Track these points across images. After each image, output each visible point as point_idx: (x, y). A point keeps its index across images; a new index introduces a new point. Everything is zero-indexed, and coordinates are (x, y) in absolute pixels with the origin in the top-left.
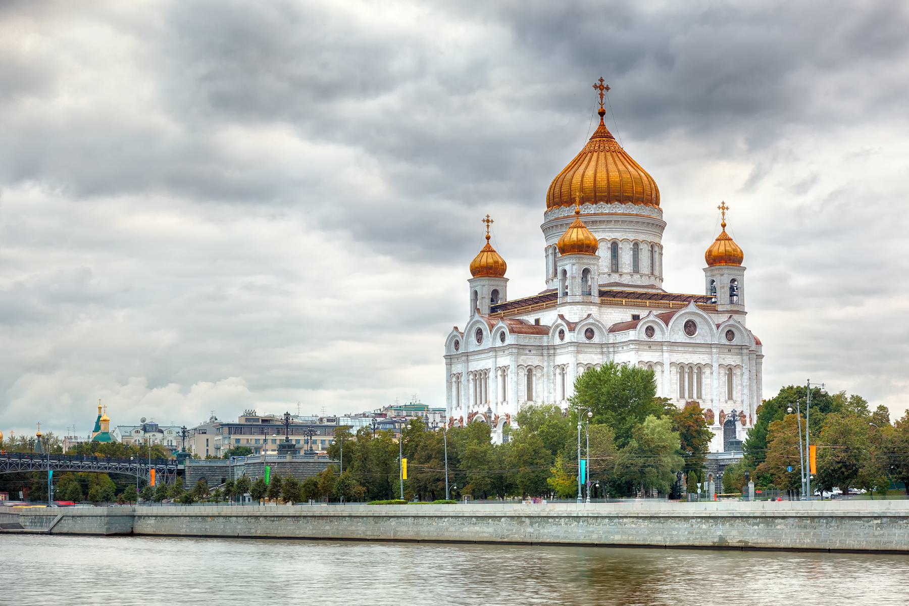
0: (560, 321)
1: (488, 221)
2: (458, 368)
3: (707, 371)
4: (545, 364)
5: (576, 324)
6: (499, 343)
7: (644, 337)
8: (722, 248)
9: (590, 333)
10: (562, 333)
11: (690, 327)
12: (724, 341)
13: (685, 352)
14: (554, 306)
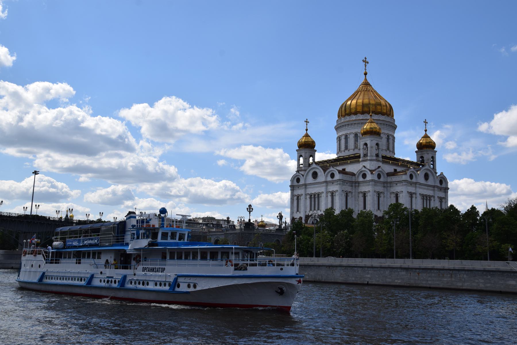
0: (364, 169)
1: (307, 122)
2: (298, 192)
3: (432, 199)
4: (354, 191)
5: (374, 170)
6: (329, 179)
7: (409, 179)
8: (424, 141)
9: (379, 176)
10: (364, 176)
11: (426, 177)
12: (439, 185)
13: (424, 189)
14: (359, 162)
